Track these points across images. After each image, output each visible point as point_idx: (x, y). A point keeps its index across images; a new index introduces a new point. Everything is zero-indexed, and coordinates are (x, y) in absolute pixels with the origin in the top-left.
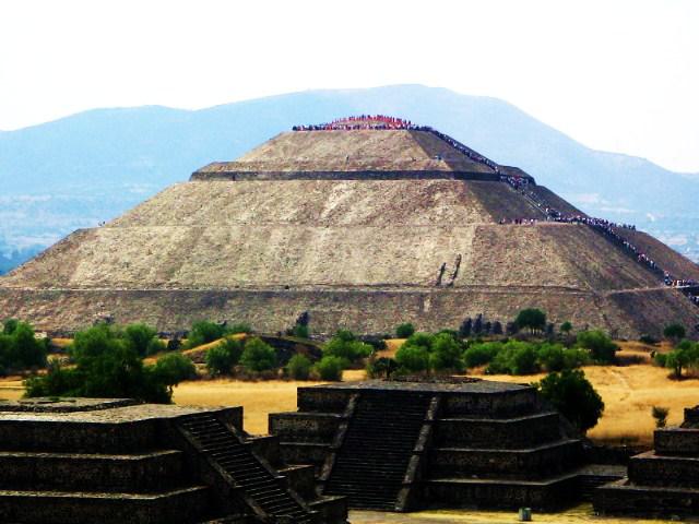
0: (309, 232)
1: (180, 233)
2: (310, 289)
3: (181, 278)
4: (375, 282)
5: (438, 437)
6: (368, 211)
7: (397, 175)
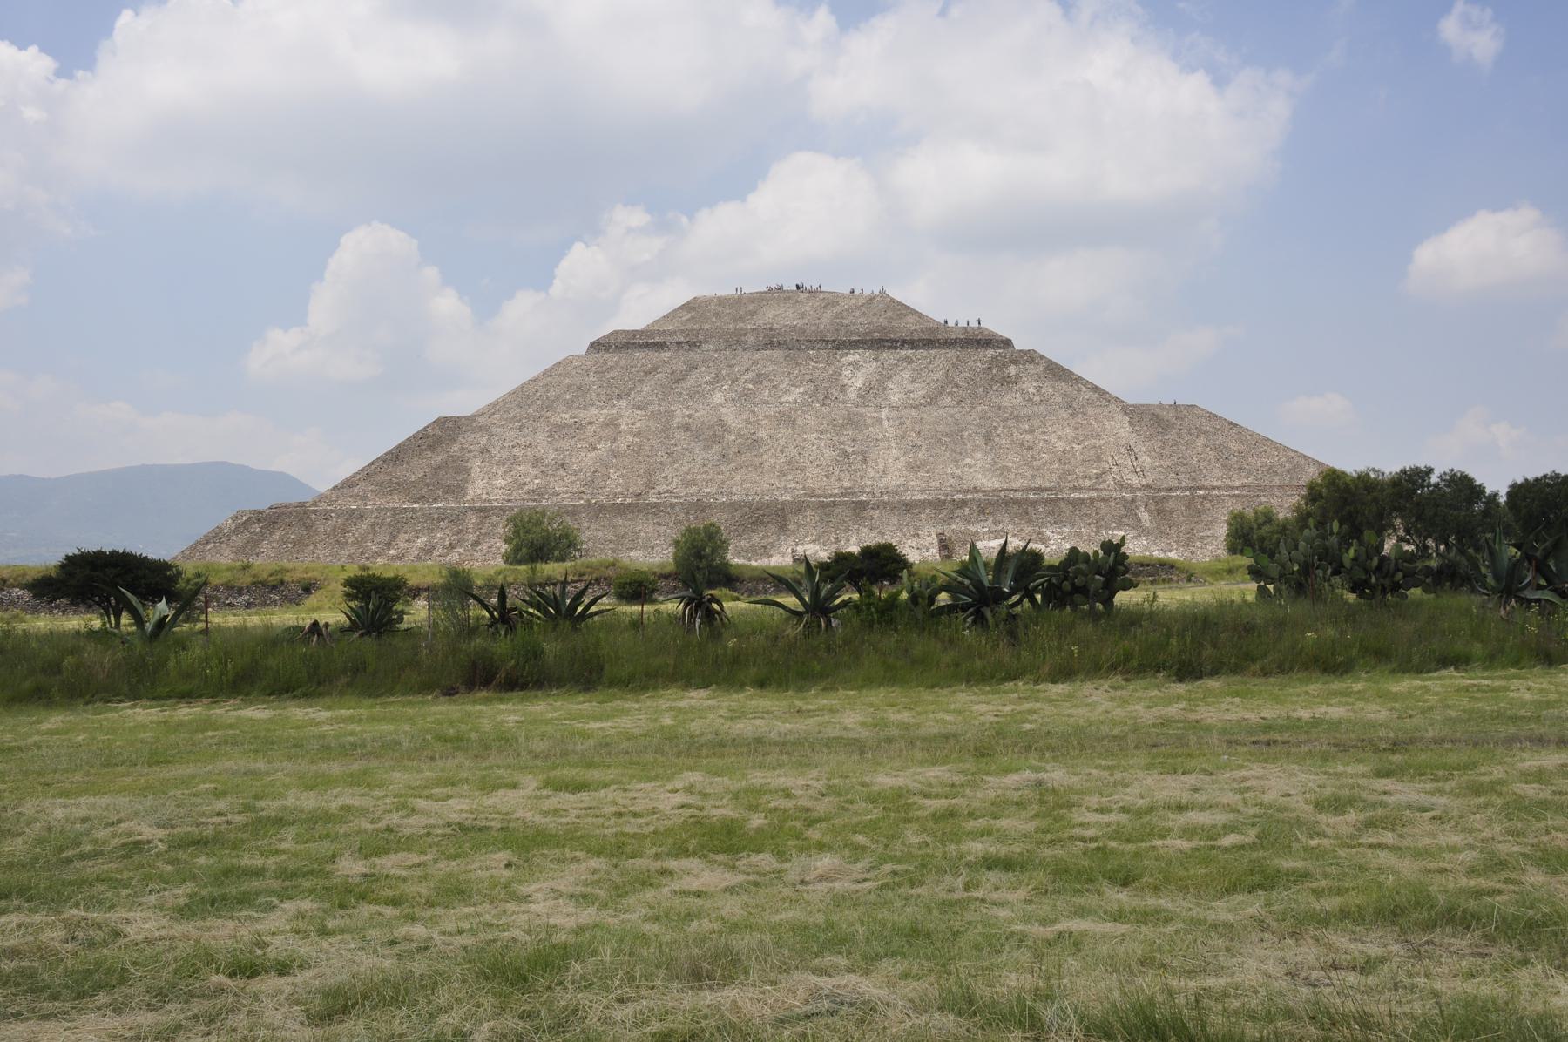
4: (1018, 484)
6: (919, 391)
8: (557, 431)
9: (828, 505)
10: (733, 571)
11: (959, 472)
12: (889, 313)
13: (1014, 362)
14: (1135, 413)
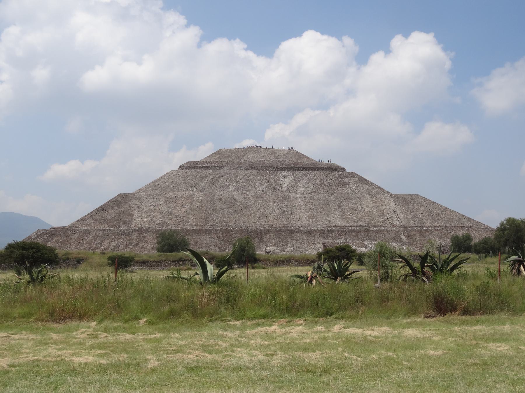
4: (352, 224)
6: (311, 187)
8: (168, 200)
9: (279, 231)
10: (257, 257)
11: (329, 219)
12: (297, 157)
13: (347, 177)
14: (396, 197)
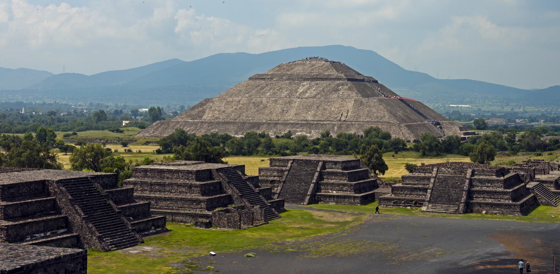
0: (293, 100)
1: (244, 100)
2: (292, 122)
3: (243, 118)
4: (316, 119)
5: (321, 177)
7: (326, 79)
